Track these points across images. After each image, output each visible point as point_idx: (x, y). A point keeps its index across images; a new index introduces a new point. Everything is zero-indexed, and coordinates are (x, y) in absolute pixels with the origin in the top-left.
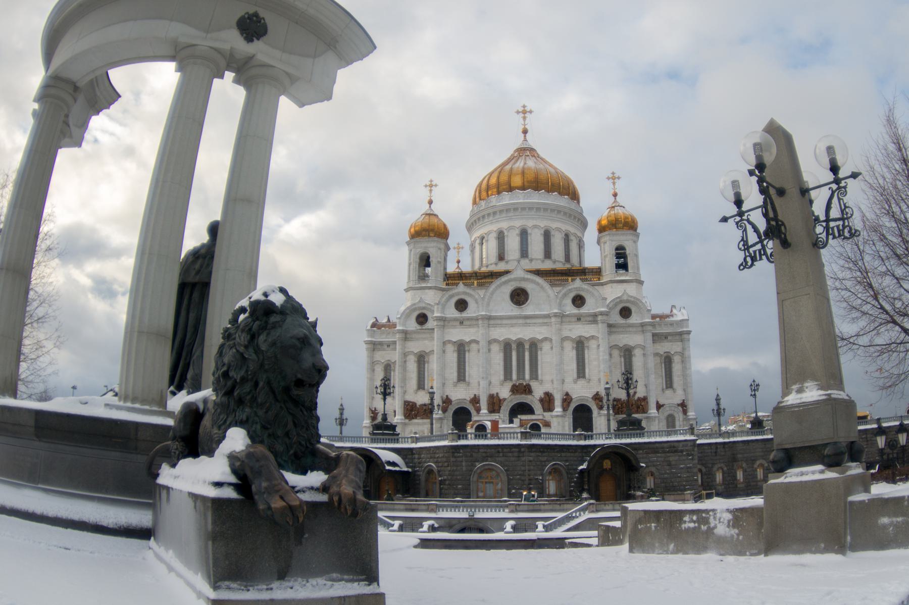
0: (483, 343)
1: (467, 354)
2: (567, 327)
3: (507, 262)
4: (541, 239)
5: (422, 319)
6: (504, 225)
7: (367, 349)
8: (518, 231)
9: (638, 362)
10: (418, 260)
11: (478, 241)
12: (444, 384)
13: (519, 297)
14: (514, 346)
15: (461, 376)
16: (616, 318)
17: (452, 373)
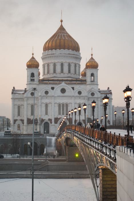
0: (53, 104)
1: (48, 107)
2: (76, 100)
3: (56, 74)
4: (68, 67)
5: (32, 94)
6: (56, 61)
7: (12, 101)
8: (60, 64)
10: (30, 75)
11: (46, 65)
12: (42, 115)
13: (63, 91)
14: (61, 105)
15: (46, 113)
16: (90, 96)
17: (44, 113)
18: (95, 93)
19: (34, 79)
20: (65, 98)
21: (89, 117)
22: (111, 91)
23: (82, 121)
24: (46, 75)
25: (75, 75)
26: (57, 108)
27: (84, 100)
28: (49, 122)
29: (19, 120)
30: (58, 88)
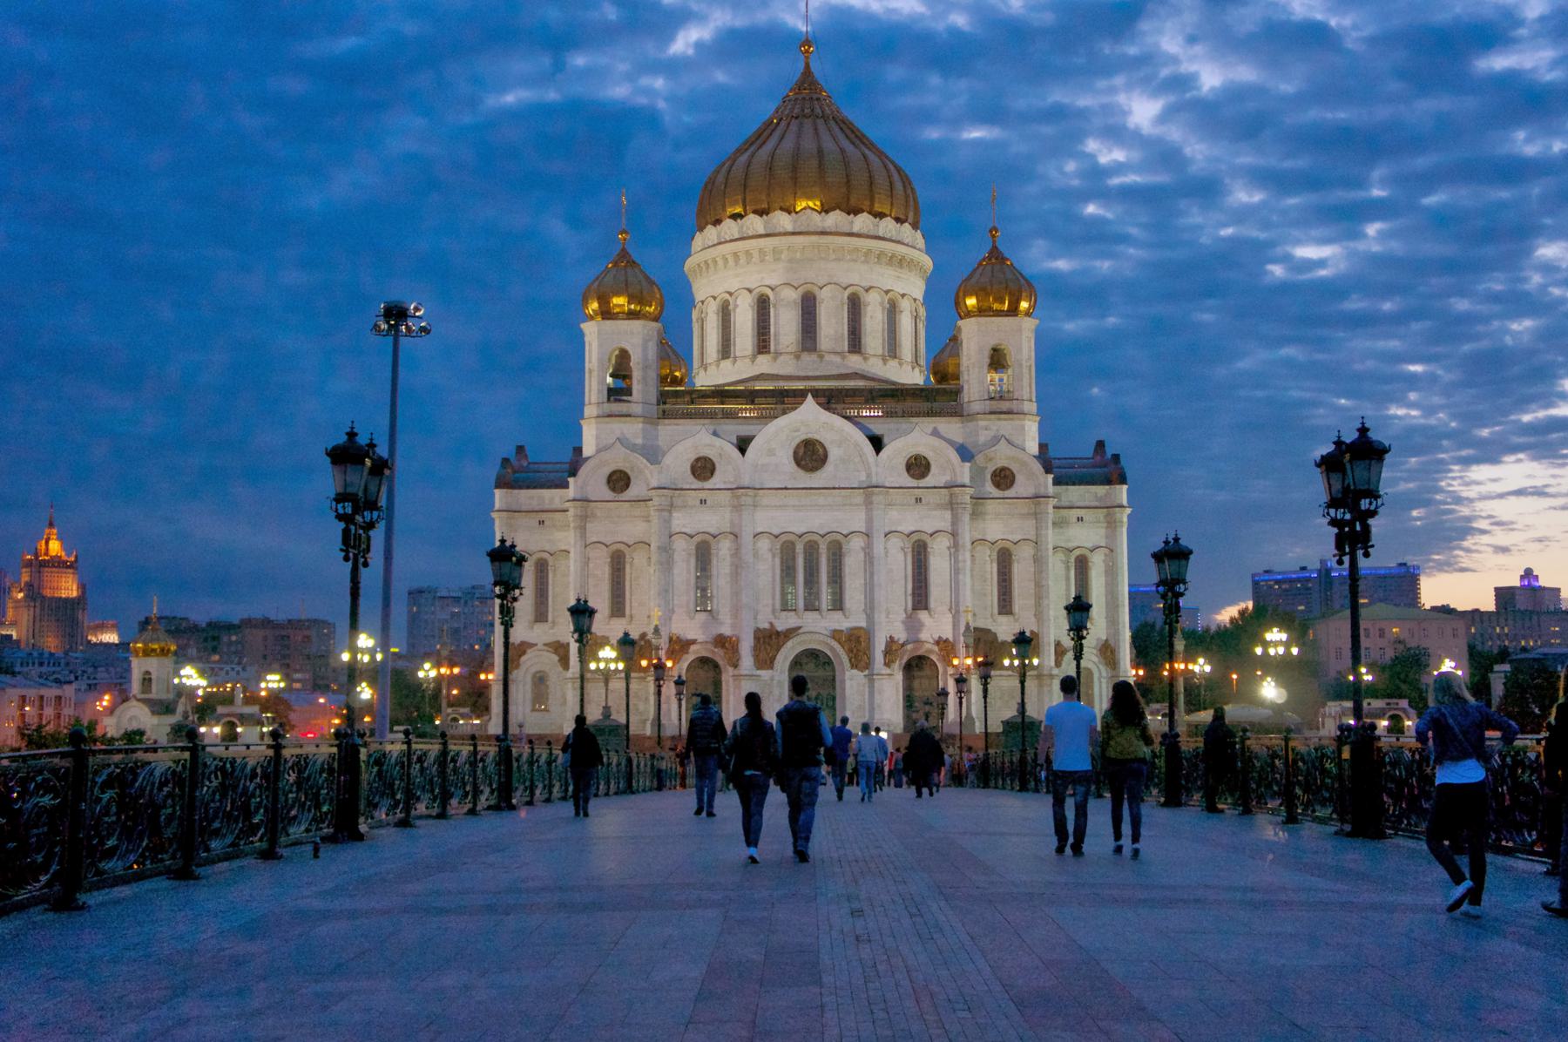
1: (714, 562)
2: (894, 514)
9: (1021, 572)
13: (810, 455)
14: (800, 548)
18: (1014, 468)
19: (629, 392)
20: (821, 501)
21: (981, 624)
22: (1116, 457)
23: (936, 648)
24: (712, 369)
25: (893, 363)
26: (766, 570)
27: (948, 515)
28: (719, 656)
29: (540, 646)
30: (777, 436)
